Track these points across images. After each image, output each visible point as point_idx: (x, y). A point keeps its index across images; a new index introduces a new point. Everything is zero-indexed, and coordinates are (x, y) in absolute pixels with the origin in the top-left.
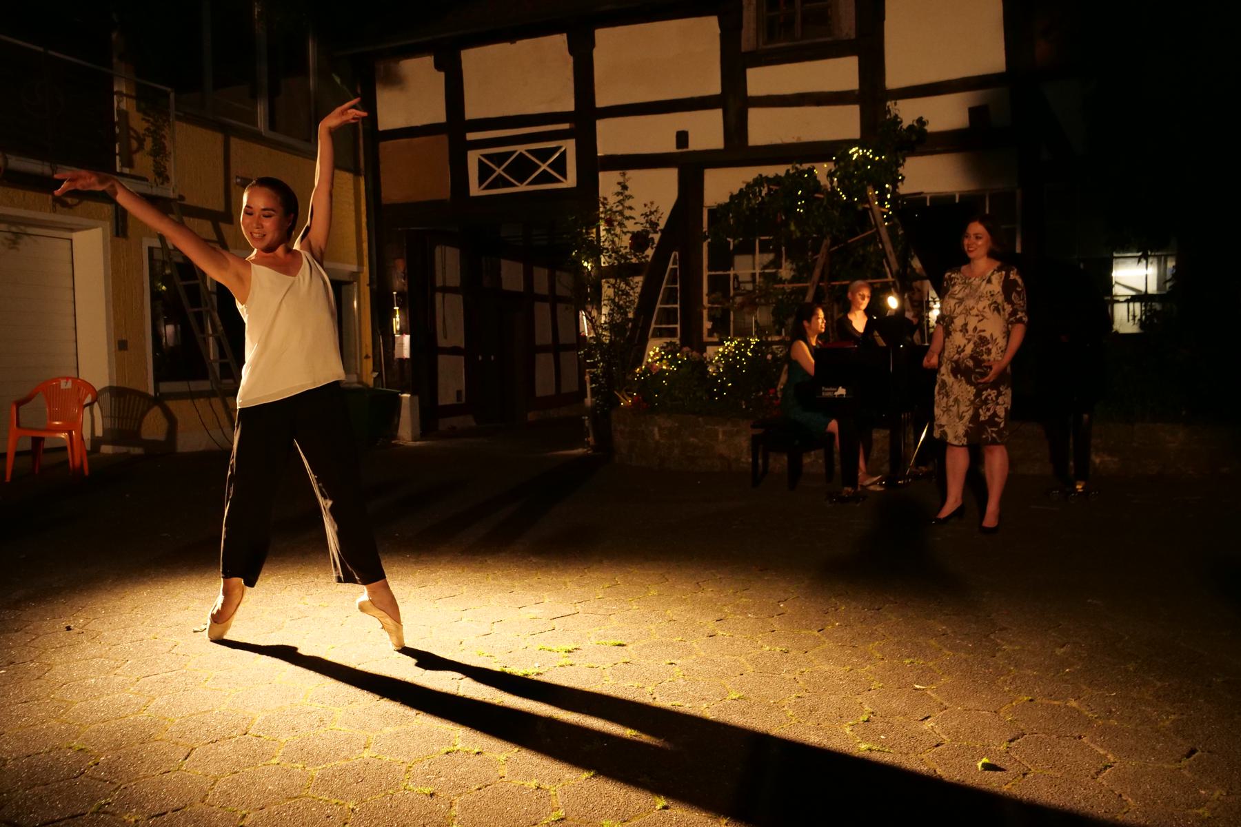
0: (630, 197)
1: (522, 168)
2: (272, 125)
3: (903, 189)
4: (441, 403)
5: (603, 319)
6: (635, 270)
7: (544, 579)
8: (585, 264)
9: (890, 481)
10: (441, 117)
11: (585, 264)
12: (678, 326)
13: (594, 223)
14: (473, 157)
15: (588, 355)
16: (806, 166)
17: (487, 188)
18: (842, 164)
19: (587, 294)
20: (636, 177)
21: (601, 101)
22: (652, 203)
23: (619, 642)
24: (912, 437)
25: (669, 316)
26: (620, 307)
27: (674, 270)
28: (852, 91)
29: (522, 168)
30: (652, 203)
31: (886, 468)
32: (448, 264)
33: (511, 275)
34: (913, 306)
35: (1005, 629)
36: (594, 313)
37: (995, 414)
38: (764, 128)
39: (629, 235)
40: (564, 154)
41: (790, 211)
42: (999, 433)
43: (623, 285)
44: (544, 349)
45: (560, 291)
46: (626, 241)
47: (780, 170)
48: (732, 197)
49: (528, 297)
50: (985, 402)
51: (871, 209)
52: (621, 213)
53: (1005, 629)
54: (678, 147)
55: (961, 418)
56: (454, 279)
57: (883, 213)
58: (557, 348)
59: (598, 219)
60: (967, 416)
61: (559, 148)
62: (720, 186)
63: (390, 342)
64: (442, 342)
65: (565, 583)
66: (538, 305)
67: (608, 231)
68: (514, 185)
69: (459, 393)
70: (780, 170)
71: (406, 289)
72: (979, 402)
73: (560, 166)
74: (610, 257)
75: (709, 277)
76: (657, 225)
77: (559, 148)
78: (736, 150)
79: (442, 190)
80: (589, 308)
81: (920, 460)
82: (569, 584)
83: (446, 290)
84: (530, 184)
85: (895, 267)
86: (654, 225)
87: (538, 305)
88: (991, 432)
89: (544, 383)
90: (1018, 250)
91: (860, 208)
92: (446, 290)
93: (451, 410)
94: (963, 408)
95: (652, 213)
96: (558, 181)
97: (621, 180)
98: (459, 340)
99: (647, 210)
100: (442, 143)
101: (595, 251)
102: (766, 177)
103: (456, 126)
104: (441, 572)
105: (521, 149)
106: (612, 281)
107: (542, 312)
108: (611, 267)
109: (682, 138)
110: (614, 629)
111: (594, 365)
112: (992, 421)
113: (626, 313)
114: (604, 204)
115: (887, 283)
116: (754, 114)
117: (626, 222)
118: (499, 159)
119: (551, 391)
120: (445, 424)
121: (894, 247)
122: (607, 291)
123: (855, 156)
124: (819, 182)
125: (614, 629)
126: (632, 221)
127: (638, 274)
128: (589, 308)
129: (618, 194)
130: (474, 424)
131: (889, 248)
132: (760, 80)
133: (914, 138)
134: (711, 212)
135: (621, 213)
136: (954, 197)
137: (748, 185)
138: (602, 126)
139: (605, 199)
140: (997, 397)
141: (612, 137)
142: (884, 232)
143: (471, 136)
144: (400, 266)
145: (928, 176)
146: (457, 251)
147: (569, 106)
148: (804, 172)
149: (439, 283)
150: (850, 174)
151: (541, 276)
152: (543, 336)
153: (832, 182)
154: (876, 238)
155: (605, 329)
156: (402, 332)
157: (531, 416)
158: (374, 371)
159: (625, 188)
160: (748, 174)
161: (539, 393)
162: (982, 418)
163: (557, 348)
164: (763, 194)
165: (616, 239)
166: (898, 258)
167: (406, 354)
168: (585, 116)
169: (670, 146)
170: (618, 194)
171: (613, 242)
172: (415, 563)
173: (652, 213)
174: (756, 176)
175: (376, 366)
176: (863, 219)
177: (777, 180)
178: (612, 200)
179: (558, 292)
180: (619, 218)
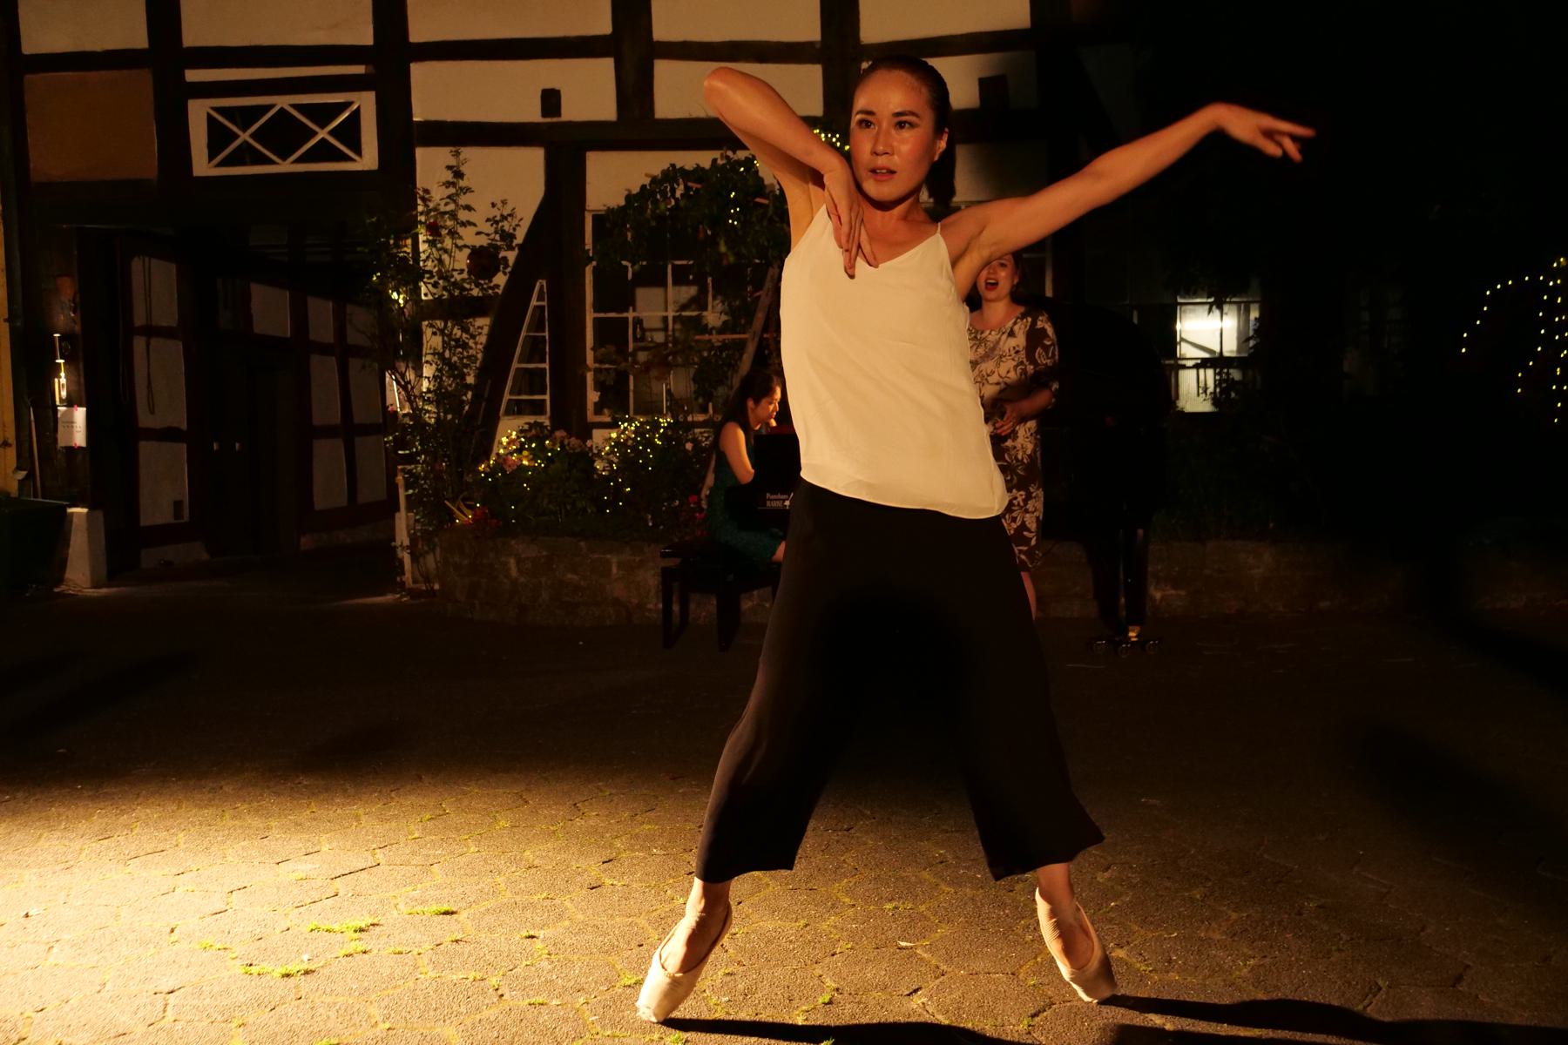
0: (468, 190)
1: (284, 135)
4: (145, 521)
5: (425, 384)
6: (477, 307)
7: (322, 813)
8: (395, 296)
10: (138, 38)
11: (395, 296)
12: (547, 397)
13: (409, 229)
14: (198, 113)
15: (401, 443)
17: (224, 163)
19: (398, 345)
20: (476, 158)
21: (420, 31)
22: (504, 202)
23: (446, 908)
25: (532, 381)
26: (452, 366)
28: (811, 44)
29: (284, 135)
30: (504, 202)
32: (156, 288)
33: (270, 310)
36: (410, 375)
37: (1023, 527)
38: (678, 91)
39: (467, 251)
40: (356, 115)
41: (718, 222)
43: (457, 332)
44: (329, 432)
45: (353, 338)
46: (462, 260)
47: (703, 159)
48: (629, 198)
49: (299, 346)
52: (453, 215)
54: (544, 115)
56: (166, 312)
58: (349, 430)
59: (416, 223)
61: (347, 105)
62: (611, 179)
63: (49, 421)
64: (145, 420)
65: (357, 818)
66: (315, 359)
67: (432, 243)
68: (272, 162)
69: (178, 505)
70: (703, 159)
71: (77, 328)
73: (350, 133)
74: (435, 285)
75: (596, 320)
76: (513, 237)
77: (347, 105)
78: (636, 125)
79: (144, 163)
80: (402, 366)
82: (364, 819)
83: (151, 331)
84: (298, 161)
86: (507, 237)
87: (315, 359)
89: (328, 489)
90: (1049, 293)
92: (151, 331)
93: (164, 534)
95: (504, 218)
96: (348, 159)
97: (453, 162)
98: (178, 417)
99: (496, 213)
100: (142, 82)
101: (410, 275)
102: (682, 169)
103: (166, 56)
104: (140, 812)
105: (283, 102)
106: (440, 324)
107: (323, 371)
108: (438, 301)
109: (551, 100)
110: (438, 887)
111: (411, 459)
113: (463, 376)
114: (423, 199)
116: (664, 70)
117: (461, 230)
118: (245, 116)
119: (342, 501)
120: (150, 558)
122: (432, 340)
124: (762, 180)
125: (438, 887)
126: (471, 229)
127: (483, 314)
128: (402, 366)
129: (448, 184)
130: (205, 556)
134: (597, 219)
135: (453, 215)
137: (654, 180)
138: (422, 74)
139: (426, 191)
140: (1026, 501)
141: (436, 92)
143: (193, 76)
144: (67, 290)
146: (173, 268)
148: (739, 163)
149: (139, 320)
151: (321, 313)
152: (326, 409)
155: (429, 401)
156: (70, 402)
157: (306, 542)
158: (19, 468)
159: (459, 175)
160: (655, 162)
161: (320, 503)
163: (349, 430)
164: (678, 195)
165: (445, 257)
167: (79, 438)
168: (391, 56)
169: (530, 112)
170: (448, 184)
171: (440, 261)
172: (94, 798)
173: (504, 218)
174: (666, 166)
175: (23, 461)
177: (698, 174)
178: (438, 195)
179: (350, 341)
180: (449, 223)
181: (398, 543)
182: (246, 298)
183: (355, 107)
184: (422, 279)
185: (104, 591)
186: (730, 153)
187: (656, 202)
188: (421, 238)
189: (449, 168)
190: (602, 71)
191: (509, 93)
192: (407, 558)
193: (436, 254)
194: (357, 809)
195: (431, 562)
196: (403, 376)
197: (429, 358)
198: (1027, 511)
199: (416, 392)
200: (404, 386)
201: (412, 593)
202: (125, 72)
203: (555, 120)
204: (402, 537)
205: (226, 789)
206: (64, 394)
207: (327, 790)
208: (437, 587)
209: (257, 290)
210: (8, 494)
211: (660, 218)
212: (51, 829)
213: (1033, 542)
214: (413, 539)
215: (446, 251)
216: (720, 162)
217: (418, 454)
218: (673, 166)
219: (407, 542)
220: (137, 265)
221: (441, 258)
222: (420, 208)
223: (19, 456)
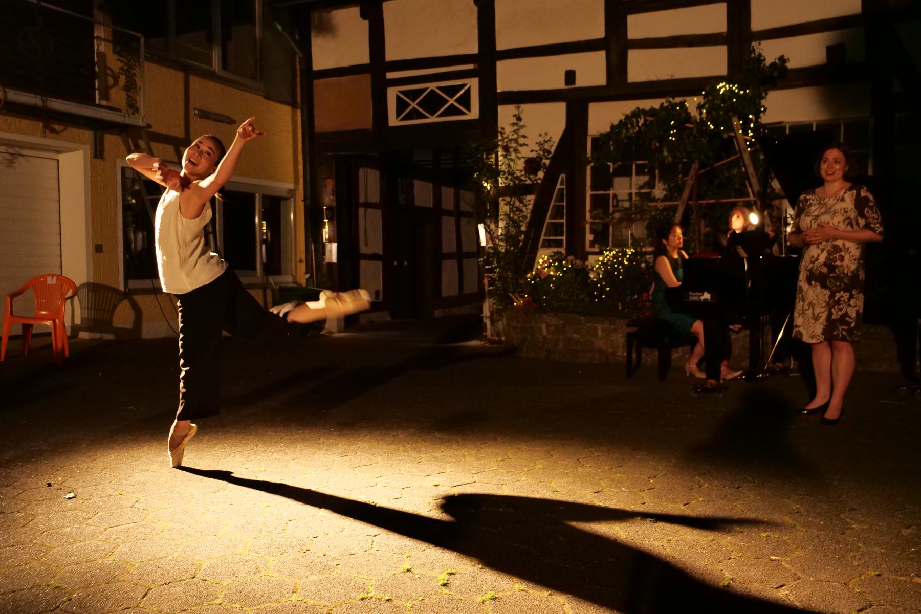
1: (433, 103)
2: (225, 65)
3: (765, 119)
5: (500, 231)
6: (528, 190)
8: (485, 184)
9: (750, 375)
10: (365, 59)
11: (485, 184)
12: (564, 238)
13: (493, 149)
14: (392, 93)
15: (487, 262)
16: (678, 100)
17: (404, 119)
18: (710, 98)
19: (486, 210)
20: (528, 110)
21: (502, 45)
24: (770, 337)
25: (556, 229)
26: (514, 222)
27: (561, 190)
28: (720, 34)
29: (433, 103)
31: (746, 364)
32: (370, 183)
33: (423, 193)
34: (771, 222)
35: (855, 509)
36: (493, 226)
37: (846, 315)
38: (642, 67)
39: (523, 160)
40: (469, 90)
41: (663, 139)
42: (850, 331)
43: (517, 203)
44: (450, 256)
45: (464, 207)
46: (520, 165)
47: (655, 104)
48: (612, 127)
49: (436, 213)
50: (838, 303)
51: (736, 137)
52: (516, 141)
53: (855, 509)
54: (567, 84)
55: (816, 318)
56: (375, 197)
57: (747, 140)
58: (460, 256)
60: (824, 316)
61: (464, 85)
62: (603, 118)
63: (321, 249)
64: (364, 250)
65: (464, 457)
66: (445, 219)
67: (505, 156)
68: (426, 117)
69: (377, 293)
70: (655, 104)
71: (334, 204)
72: (833, 303)
73: (465, 100)
74: (506, 178)
75: (592, 196)
77: (464, 85)
78: (617, 86)
79: (366, 121)
80: (488, 221)
81: (777, 357)
82: (467, 457)
83: (367, 205)
84: (440, 116)
85: (757, 187)
87: (445, 219)
88: (842, 330)
89: (449, 287)
90: (870, 172)
91: (725, 136)
92: (367, 205)
94: (818, 310)
96: (463, 113)
97: (516, 112)
98: (378, 249)
100: (366, 80)
101: (493, 173)
102: (643, 110)
103: (378, 66)
104: (360, 444)
105: (433, 86)
106: (508, 199)
107: (448, 224)
108: (508, 187)
109: (570, 76)
111: (491, 271)
112: (843, 320)
113: (519, 227)
114: (502, 133)
115: (749, 201)
116: (633, 56)
117: (520, 149)
118: (413, 95)
119: (454, 292)
121: (756, 170)
122: (504, 208)
123: (722, 91)
124: (689, 114)
127: (530, 193)
128: (488, 221)
129: (514, 124)
130: (389, 319)
131: (751, 170)
132: (639, 25)
133: (776, 74)
134: (595, 140)
135: (516, 141)
136: (812, 125)
137: (627, 117)
138: (502, 66)
139: (503, 129)
140: (849, 299)
141: (510, 75)
142: (747, 158)
143: (390, 75)
144: (330, 185)
145: (787, 108)
147: (474, 49)
148: (677, 105)
149: (362, 200)
150: (719, 108)
151: (448, 193)
152: (449, 244)
153: (701, 113)
154: (739, 162)
157: (438, 313)
158: (307, 273)
159: (519, 119)
160: (626, 107)
161: (445, 294)
162: (834, 317)
163: (460, 256)
164: (640, 124)
165: (512, 163)
166: (759, 180)
167: (334, 259)
168: (487, 58)
169: (559, 83)
170: (514, 124)
171: (509, 165)
174: (634, 108)
175: (309, 269)
176: (728, 145)
177: (652, 112)
178: (509, 130)
180: (514, 145)
181: (484, 315)
182: (412, 187)
183: (467, 87)
184: (499, 175)
185: (343, 334)
186: (671, 99)
187: (628, 129)
188: (500, 154)
189: (515, 116)
192: (488, 322)
193: (507, 162)
194: (464, 452)
195: (500, 325)
196: (489, 227)
197: (502, 217)
198: (849, 305)
199: (495, 235)
200: (488, 232)
201: (490, 341)
202: (358, 76)
204: (486, 312)
205: (401, 436)
206: (327, 236)
207: (449, 441)
208: (503, 339)
209: (418, 184)
210: (301, 285)
211: (629, 138)
212: (320, 449)
213: (853, 325)
214: (492, 313)
215: (512, 160)
216: (665, 105)
217: (496, 268)
218: (638, 108)
219: (488, 314)
220: (361, 172)
221: (510, 164)
222: (500, 138)
223: (307, 267)
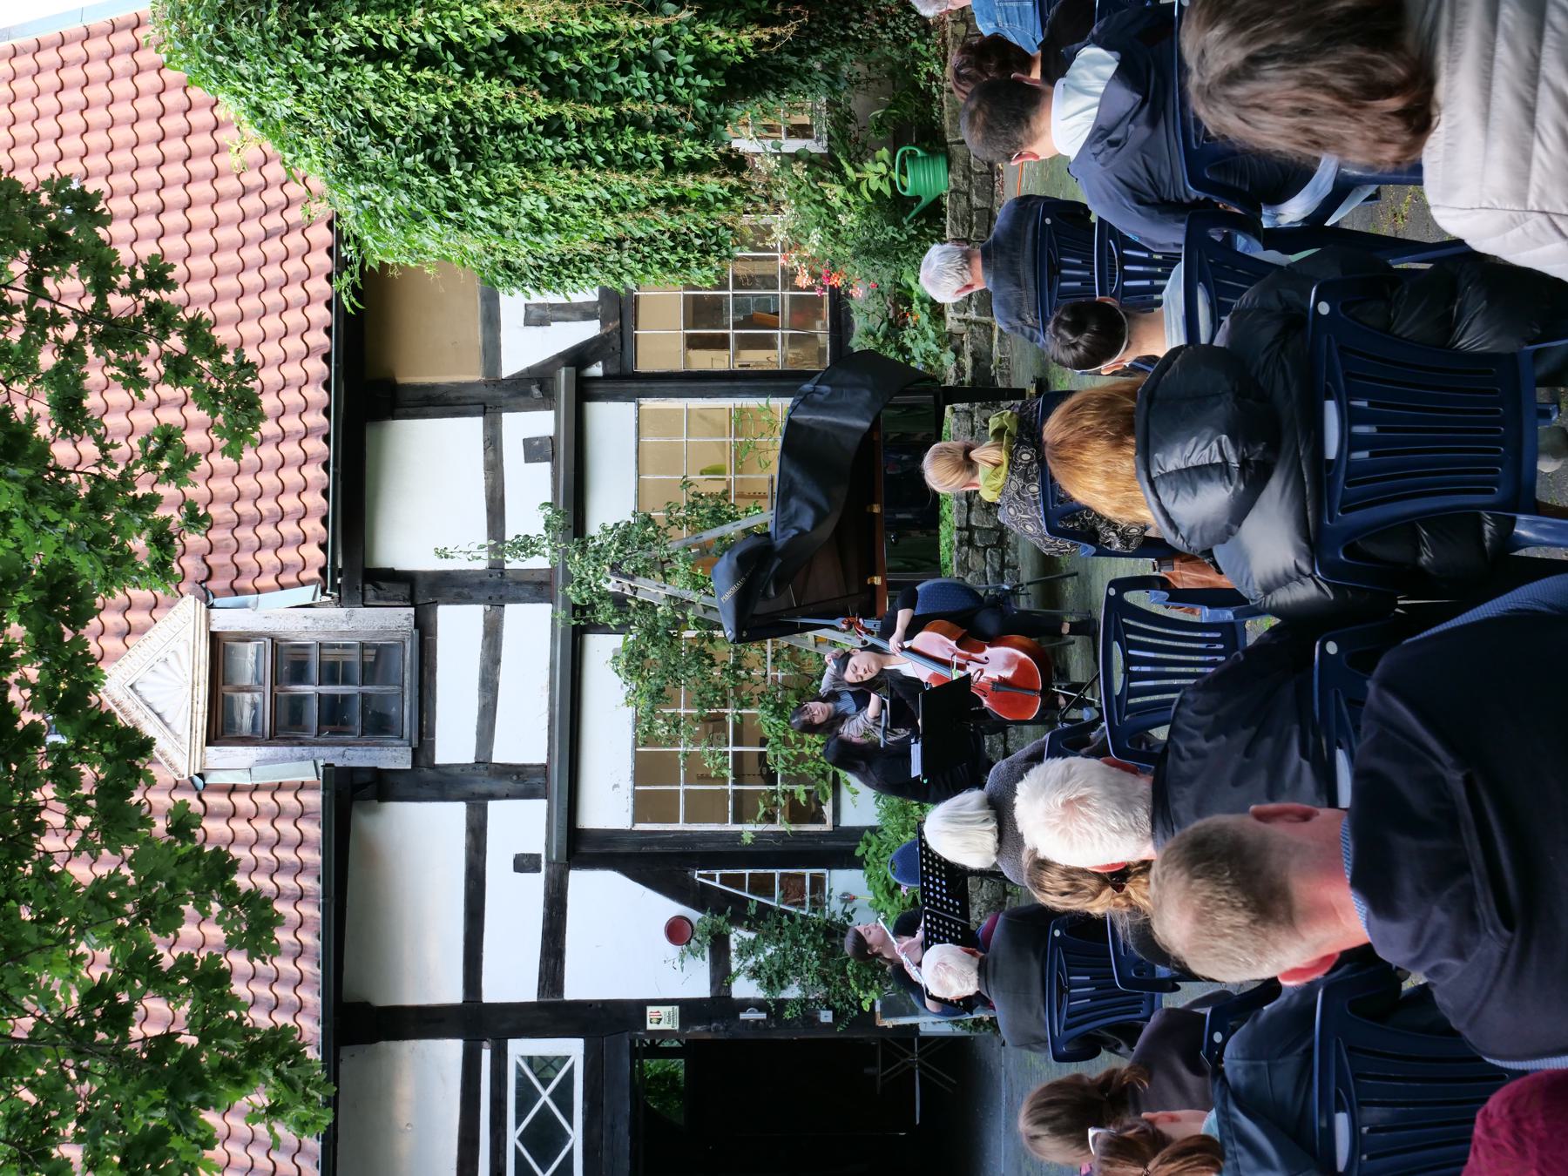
25: (792, 888)
40: (530, 1060)
54: (538, 870)
61: (518, 1065)
73: (544, 1066)
84: (571, 1123)
96: (571, 1071)
105: (513, 1135)
109: (525, 863)
138: (493, 993)
141: (511, 978)
168: (477, 1022)
169: (536, 883)
190: (500, 813)
191: (515, 905)
203: (543, 859)
